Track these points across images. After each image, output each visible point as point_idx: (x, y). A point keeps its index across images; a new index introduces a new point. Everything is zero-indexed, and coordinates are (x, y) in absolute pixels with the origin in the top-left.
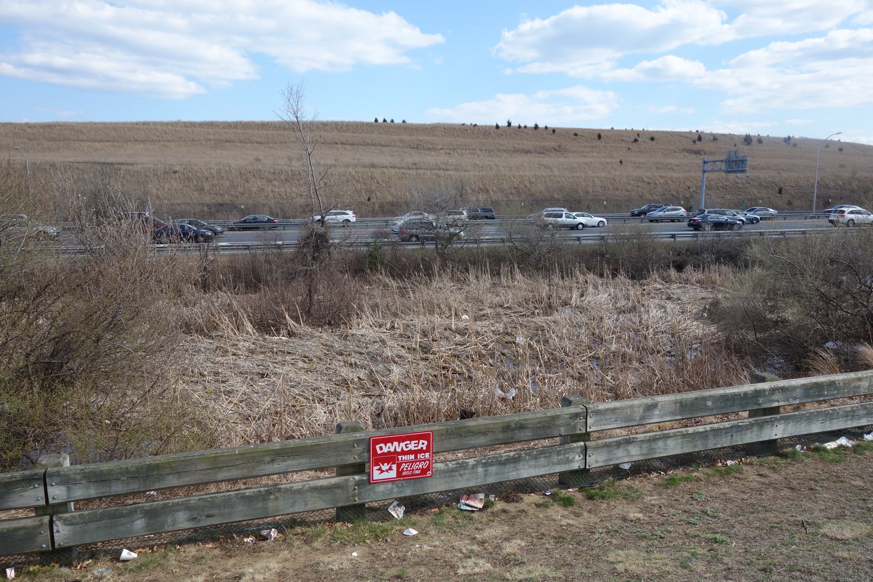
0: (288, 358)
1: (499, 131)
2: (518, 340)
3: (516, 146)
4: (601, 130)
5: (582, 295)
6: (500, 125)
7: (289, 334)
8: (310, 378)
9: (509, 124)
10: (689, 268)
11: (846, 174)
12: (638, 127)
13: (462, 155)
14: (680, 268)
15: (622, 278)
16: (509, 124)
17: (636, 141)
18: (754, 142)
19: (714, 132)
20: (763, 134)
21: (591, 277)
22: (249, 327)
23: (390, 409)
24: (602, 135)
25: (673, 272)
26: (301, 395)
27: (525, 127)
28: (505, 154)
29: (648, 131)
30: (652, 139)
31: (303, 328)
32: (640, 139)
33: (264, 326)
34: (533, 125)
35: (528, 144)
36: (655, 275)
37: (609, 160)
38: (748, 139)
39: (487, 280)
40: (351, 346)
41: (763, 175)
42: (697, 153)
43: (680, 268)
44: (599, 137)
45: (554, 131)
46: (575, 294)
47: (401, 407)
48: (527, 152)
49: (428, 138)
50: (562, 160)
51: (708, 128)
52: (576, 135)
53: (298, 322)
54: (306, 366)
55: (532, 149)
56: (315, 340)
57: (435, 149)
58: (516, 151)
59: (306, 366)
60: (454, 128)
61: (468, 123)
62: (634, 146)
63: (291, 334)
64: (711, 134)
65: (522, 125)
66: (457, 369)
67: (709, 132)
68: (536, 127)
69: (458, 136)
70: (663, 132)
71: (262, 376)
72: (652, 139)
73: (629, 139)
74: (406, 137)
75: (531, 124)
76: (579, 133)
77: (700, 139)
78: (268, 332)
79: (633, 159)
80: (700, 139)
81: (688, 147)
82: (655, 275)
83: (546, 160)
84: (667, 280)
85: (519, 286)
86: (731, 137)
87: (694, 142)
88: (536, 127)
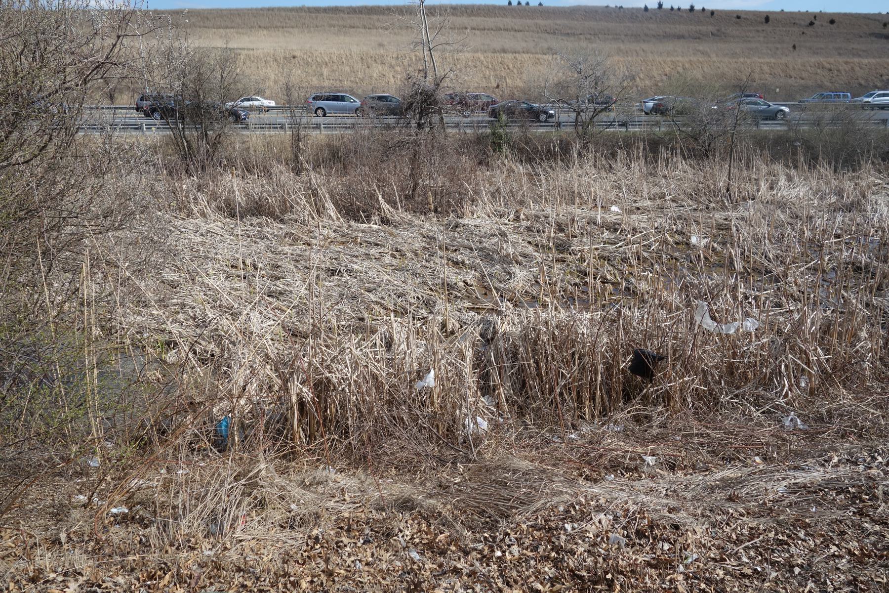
0: (373, 251)
2: (694, 240)
3: (667, 30)
4: (770, 12)
5: (772, 188)
6: (649, 7)
7: (382, 222)
8: (396, 279)
9: (660, 6)
15: (823, 169)
16: (660, 6)
17: (812, 24)
21: (778, 168)
22: (332, 210)
23: (506, 336)
24: (771, 17)
26: (378, 303)
27: (679, 9)
31: (400, 215)
32: (816, 22)
33: (354, 210)
34: (688, 7)
35: (681, 29)
39: (638, 167)
40: (460, 238)
44: (767, 19)
45: (712, 13)
46: (764, 186)
47: (525, 338)
52: (738, 17)
53: (393, 204)
54: (395, 262)
56: (414, 231)
57: (574, 34)
59: (395, 262)
60: (596, 11)
61: (612, 5)
62: (810, 31)
63: (385, 221)
65: (676, 7)
66: (609, 277)
68: (692, 9)
69: (601, 20)
71: (333, 272)
73: (803, 23)
74: (541, 22)
75: (686, 6)
76: (743, 16)
78: (357, 219)
81: (877, 31)
85: (680, 174)
88: (692, 9)
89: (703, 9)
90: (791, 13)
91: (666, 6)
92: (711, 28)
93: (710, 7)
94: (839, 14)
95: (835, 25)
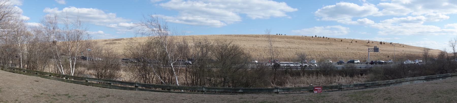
10: (364, 75)
11: (403, 53)
12: (352, 38)
14: (362, 75)
20: (385, 42)
25: (360, 75)
35: (321, 42)
36: (356, 76)
38: (381, 43)
41: (384, 52)
42: (368, 46)
43: (362, 75)
51: (371, 39)
58: (318, 44)
61: (304, 36)
62: (351, 44)
74: (286, 39)
82: (356, 76)
83: (327, 47)
84: (359, 77)
86: (377, 42)
93: (328, 37)
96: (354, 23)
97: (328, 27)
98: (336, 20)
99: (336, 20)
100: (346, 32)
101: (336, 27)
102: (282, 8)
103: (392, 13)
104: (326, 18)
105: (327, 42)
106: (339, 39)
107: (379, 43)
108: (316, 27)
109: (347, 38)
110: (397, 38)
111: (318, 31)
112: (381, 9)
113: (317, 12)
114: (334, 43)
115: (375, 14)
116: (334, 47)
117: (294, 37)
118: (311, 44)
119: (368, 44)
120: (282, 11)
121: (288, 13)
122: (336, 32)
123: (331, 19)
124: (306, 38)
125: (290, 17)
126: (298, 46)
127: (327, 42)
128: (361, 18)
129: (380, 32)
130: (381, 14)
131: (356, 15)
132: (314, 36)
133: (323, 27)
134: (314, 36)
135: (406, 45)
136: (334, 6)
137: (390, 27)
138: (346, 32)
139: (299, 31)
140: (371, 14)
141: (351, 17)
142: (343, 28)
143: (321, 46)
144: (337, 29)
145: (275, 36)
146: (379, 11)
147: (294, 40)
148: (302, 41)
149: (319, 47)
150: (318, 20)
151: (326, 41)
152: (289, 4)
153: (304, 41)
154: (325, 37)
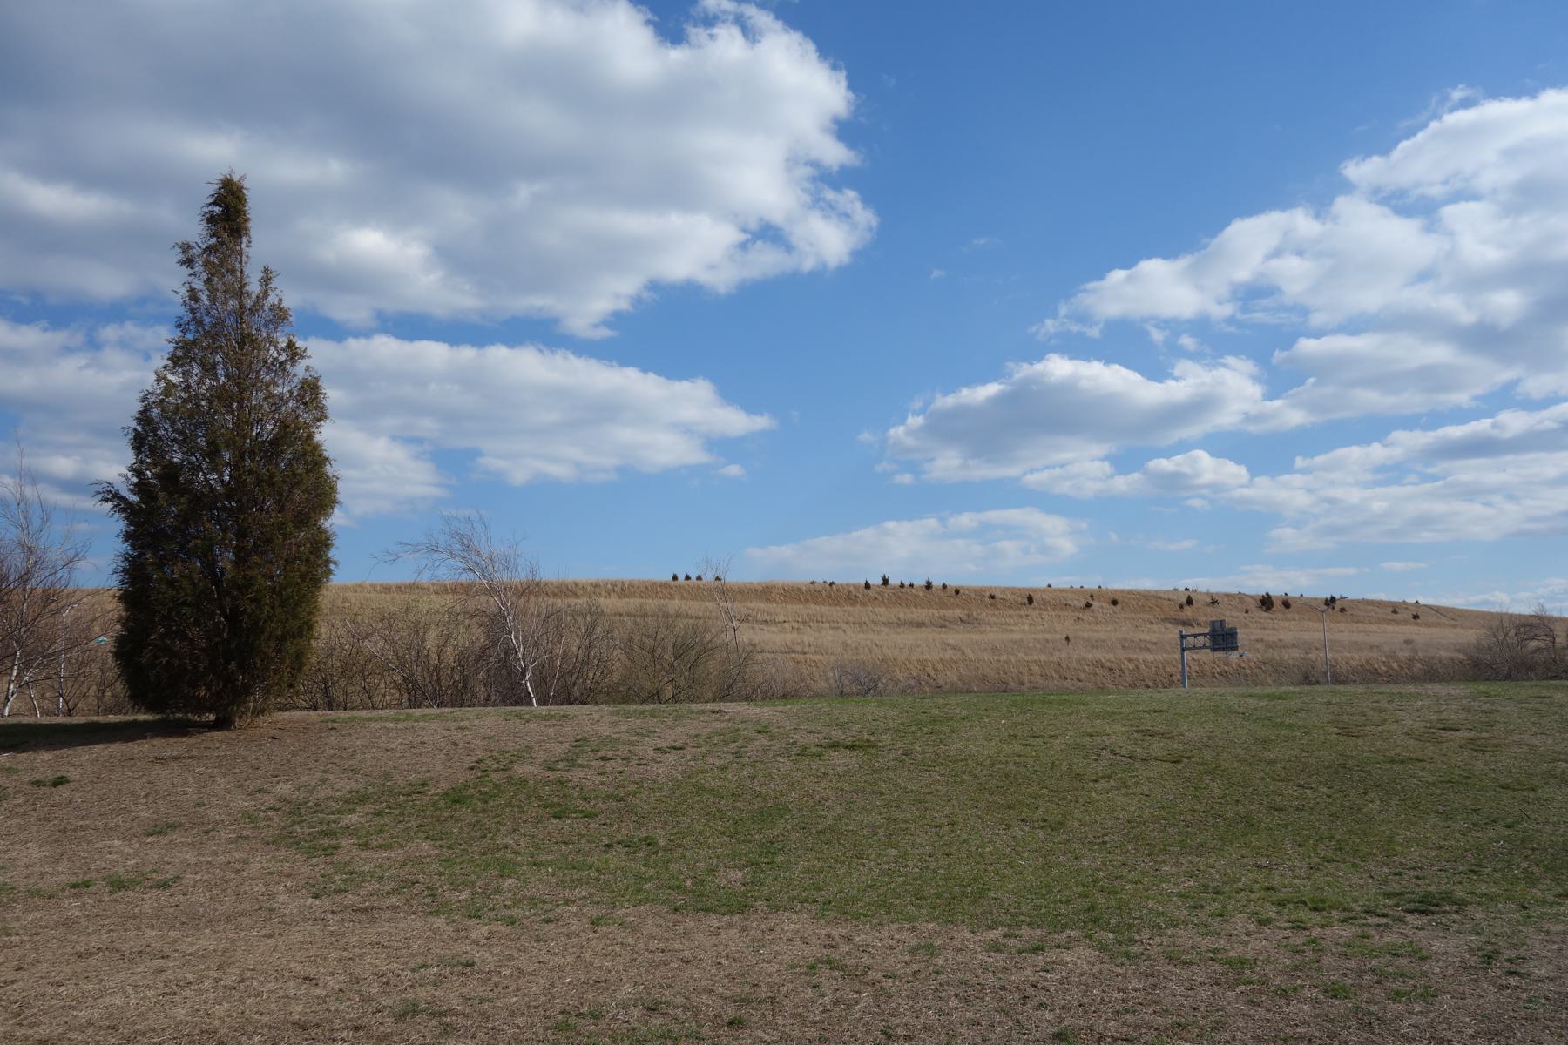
1: (871, 593)
3: (901, 615)
4: (1035, 590)
12: (1091, 583)
13: (819, 630)
17: (1088, 605)
18: (1278, 605)
19: (1213, 590)
20: (1293, 594)
24: (1035, 597)
28: (886, 630)
29: (1107, 591)
30: (1114, 603)
32: (1095, 604)
37: (1048, 636)
38: (1266, 602)
44: (1030, 600)
48: (921, 625)
49: (762, 606)
50: (975, 637)
51: (1205, 583)
52: (992, 597)
55: (927, 621)
57: (775, 622)
58: (901, 623)
61: (820, 580)
62: (1086, 616)
64: (1208, 594)
67: (1204, 590)
69: (807, 601)
70: (1130, 592)
72: (1114, 603)
73: (1078, 604)
76: (998, 595)
77: (1190, 602)
79: (1086, 635)
80: (1190, 602)
83: (952, 638)
86: (1240, 597)
87: (1181, 607)
89: (944, 586)
90: (1061, 591)
91: (894, 581)
92: (958, 612)
93: (953, 583)
94: (1122, 591)
95: (1119, 607)
96: (1122, 484)
97: (966, 520)
98: (1012, 471)
99: (1012, 471)
100: (1067, 546)
101: (1014, 515)
102: (690, 413)
103: (1370, 399)
104: (948, 463)
105: (949, 613)
106: (1013, 591)
107: (1252, 606)
108: (891, 525)
109: (1061, 582)
110: (1398, 566)
111: (903, 550)
112: (1277, 382)
113: (897, 432)
114: (984, 615)
115: (1248, 418)
116: (994, 636)
117: (765, 592)
118: (861, 624)
119: (1189, 612)
120: (686, 429)
121: (720, 445)
122: (1008, 546)
123: (983, 471)
124: (829, 594)
125: (734, 470)
126: (790, 637)
127: (949, 613)
128: (1168, 453)
129: (1288, 531)
130: (1291, 415)
131: (1134, 437)
132: (876, 581)
133: (932, 523)
134: (876, 581)
135: (1437, 610)
136: (992, 389)
137: (1354, 496)
138: (1067, 546)
139: (786, 551)
140: (1226, 418)
141: (1099, 449)
142: (1053, 527)
143: (924, 635)
144: (1011, 531)
145: (664, 585)
146: (1270, 396)
147: (772, 607)
148: (813, 608)
149: (908, 637)
150: (907, 479)
151: (942, 605)
152: (729, 394)
153: (824, 609)
154: (937, 583)
